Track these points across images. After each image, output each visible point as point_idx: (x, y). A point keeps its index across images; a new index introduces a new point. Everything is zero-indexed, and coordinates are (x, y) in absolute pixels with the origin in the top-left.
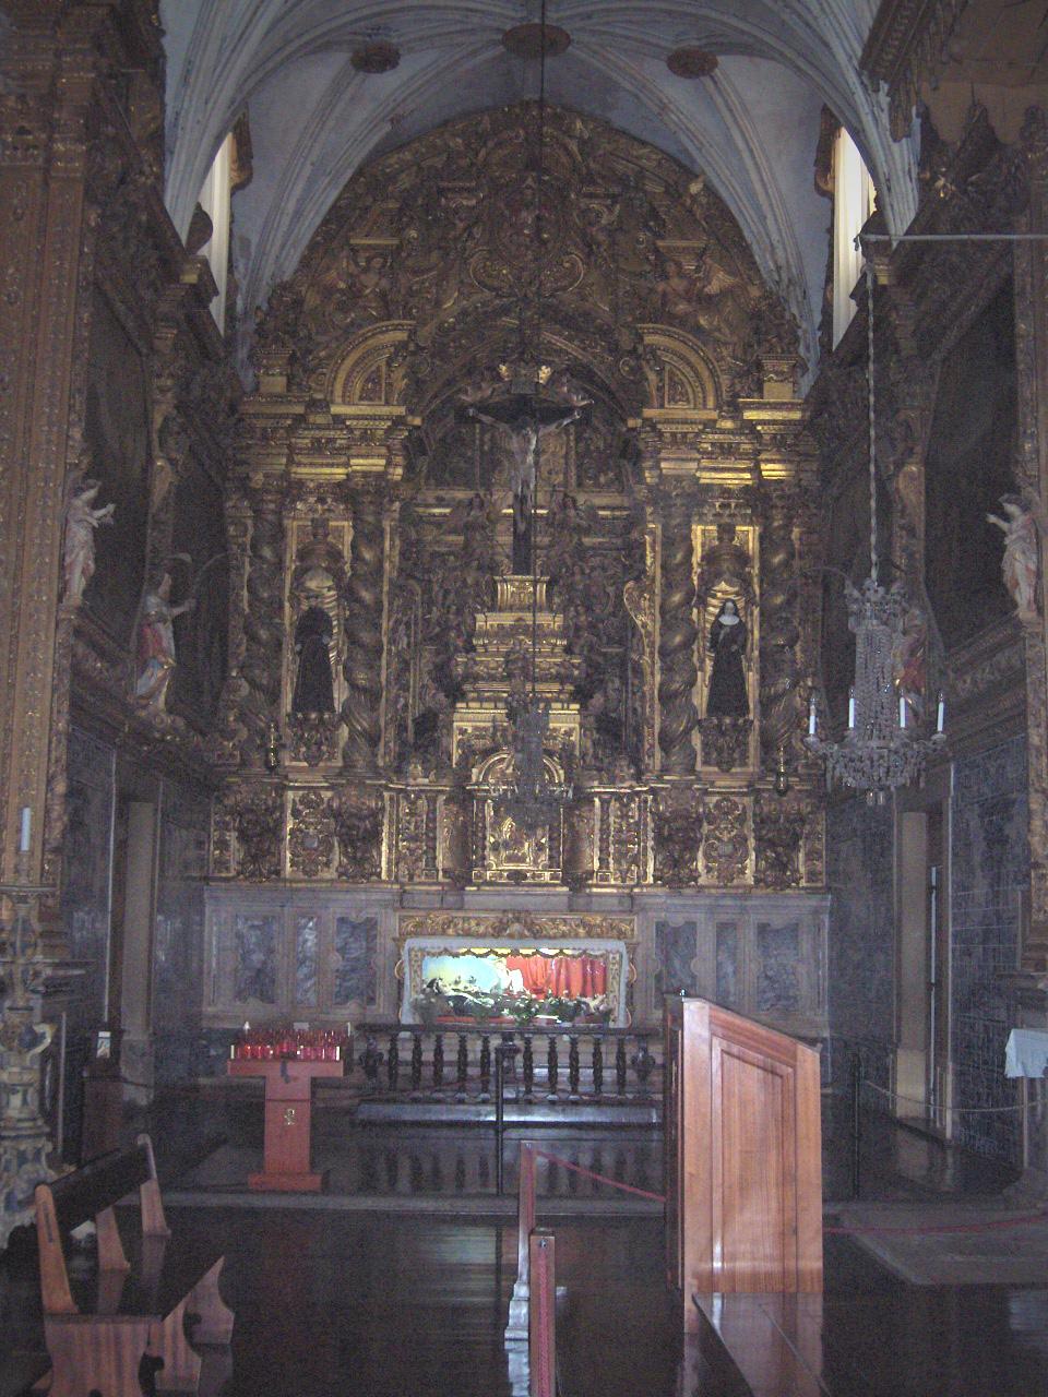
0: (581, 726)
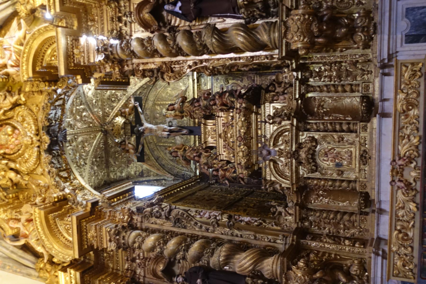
0: (271, 103)
